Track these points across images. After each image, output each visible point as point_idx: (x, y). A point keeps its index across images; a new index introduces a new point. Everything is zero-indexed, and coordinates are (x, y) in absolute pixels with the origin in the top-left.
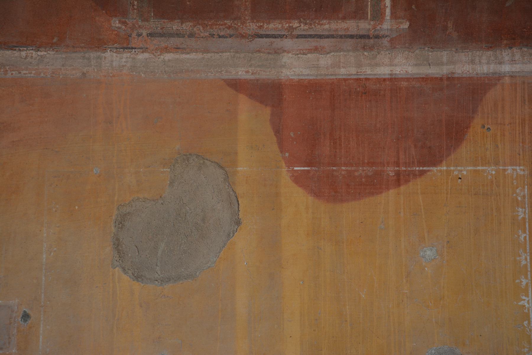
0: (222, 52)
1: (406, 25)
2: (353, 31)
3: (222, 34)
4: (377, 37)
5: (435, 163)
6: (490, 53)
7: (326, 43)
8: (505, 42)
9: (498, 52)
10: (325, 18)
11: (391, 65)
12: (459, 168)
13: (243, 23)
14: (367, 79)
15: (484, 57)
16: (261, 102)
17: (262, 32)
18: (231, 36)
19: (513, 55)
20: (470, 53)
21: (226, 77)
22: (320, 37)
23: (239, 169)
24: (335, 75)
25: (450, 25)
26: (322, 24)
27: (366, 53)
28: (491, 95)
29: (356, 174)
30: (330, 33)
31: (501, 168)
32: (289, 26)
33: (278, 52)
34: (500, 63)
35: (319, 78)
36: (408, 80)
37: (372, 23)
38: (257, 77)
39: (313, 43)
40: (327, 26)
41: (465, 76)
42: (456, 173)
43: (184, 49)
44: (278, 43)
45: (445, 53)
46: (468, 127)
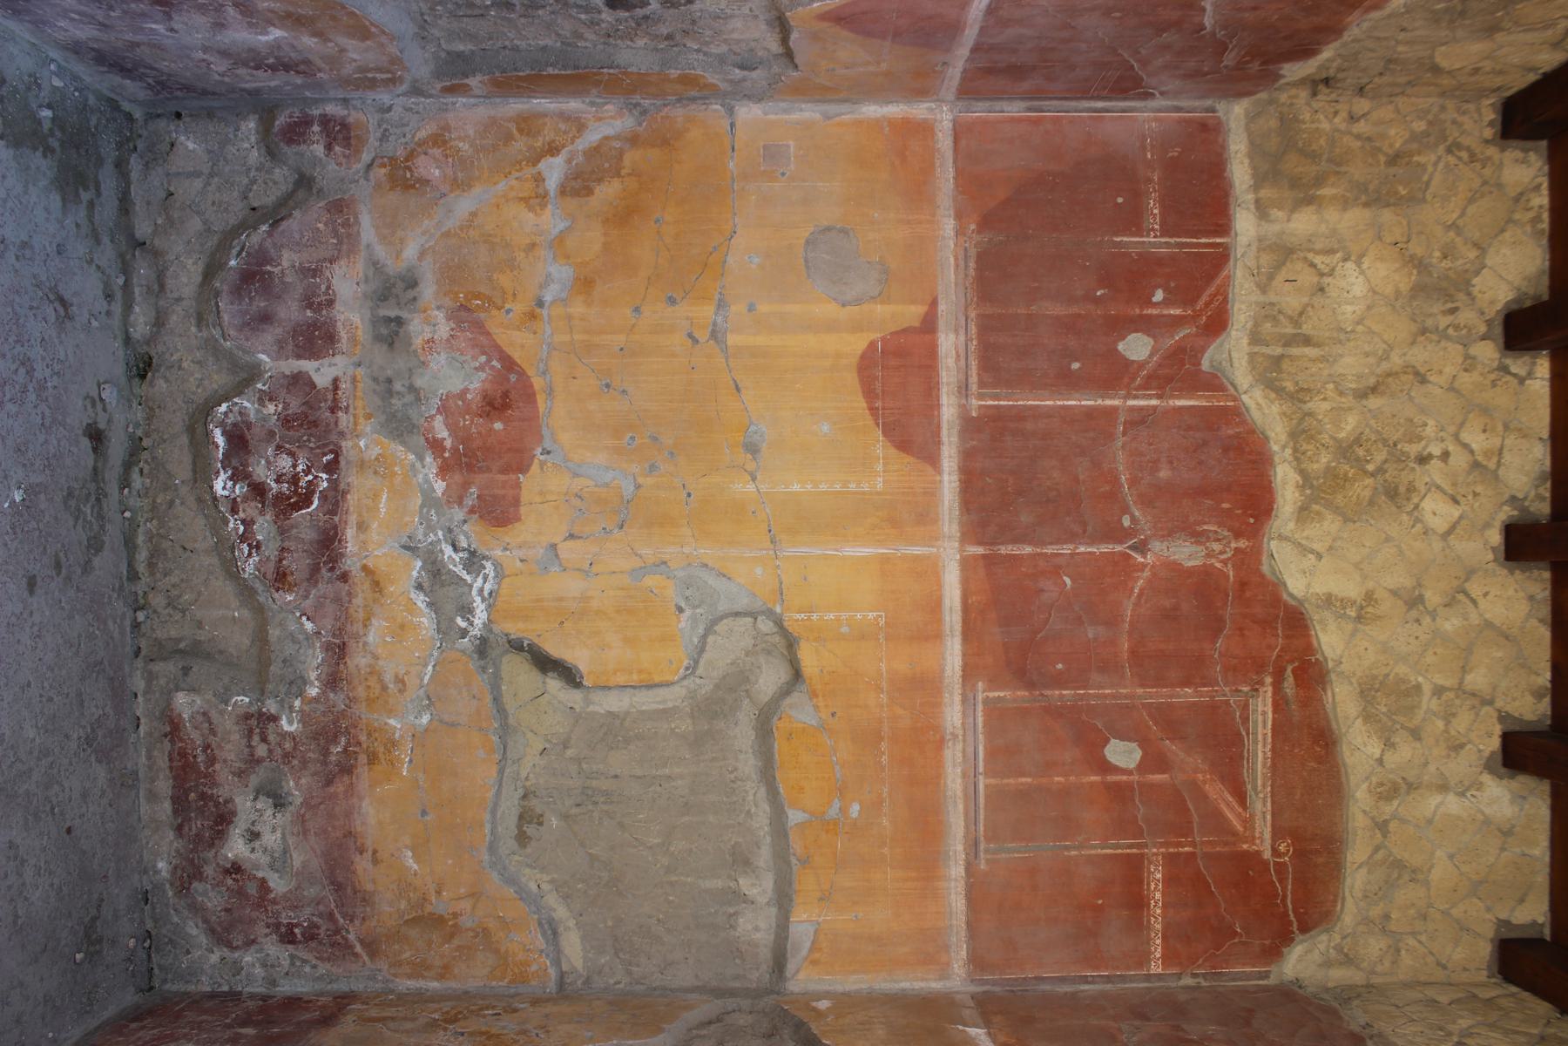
1: (974, 414)
2: (970, 380)
4: (967, 396)
5: (884, 433)
6: (956, 468)
7: (963, 362)
17: (969, 321)
18: (966, 301)
22: (967, 359)
23: (879, 306)
28: (930, 469)
33: (956, 331)
39: (962, 354)
44: (962, 331)
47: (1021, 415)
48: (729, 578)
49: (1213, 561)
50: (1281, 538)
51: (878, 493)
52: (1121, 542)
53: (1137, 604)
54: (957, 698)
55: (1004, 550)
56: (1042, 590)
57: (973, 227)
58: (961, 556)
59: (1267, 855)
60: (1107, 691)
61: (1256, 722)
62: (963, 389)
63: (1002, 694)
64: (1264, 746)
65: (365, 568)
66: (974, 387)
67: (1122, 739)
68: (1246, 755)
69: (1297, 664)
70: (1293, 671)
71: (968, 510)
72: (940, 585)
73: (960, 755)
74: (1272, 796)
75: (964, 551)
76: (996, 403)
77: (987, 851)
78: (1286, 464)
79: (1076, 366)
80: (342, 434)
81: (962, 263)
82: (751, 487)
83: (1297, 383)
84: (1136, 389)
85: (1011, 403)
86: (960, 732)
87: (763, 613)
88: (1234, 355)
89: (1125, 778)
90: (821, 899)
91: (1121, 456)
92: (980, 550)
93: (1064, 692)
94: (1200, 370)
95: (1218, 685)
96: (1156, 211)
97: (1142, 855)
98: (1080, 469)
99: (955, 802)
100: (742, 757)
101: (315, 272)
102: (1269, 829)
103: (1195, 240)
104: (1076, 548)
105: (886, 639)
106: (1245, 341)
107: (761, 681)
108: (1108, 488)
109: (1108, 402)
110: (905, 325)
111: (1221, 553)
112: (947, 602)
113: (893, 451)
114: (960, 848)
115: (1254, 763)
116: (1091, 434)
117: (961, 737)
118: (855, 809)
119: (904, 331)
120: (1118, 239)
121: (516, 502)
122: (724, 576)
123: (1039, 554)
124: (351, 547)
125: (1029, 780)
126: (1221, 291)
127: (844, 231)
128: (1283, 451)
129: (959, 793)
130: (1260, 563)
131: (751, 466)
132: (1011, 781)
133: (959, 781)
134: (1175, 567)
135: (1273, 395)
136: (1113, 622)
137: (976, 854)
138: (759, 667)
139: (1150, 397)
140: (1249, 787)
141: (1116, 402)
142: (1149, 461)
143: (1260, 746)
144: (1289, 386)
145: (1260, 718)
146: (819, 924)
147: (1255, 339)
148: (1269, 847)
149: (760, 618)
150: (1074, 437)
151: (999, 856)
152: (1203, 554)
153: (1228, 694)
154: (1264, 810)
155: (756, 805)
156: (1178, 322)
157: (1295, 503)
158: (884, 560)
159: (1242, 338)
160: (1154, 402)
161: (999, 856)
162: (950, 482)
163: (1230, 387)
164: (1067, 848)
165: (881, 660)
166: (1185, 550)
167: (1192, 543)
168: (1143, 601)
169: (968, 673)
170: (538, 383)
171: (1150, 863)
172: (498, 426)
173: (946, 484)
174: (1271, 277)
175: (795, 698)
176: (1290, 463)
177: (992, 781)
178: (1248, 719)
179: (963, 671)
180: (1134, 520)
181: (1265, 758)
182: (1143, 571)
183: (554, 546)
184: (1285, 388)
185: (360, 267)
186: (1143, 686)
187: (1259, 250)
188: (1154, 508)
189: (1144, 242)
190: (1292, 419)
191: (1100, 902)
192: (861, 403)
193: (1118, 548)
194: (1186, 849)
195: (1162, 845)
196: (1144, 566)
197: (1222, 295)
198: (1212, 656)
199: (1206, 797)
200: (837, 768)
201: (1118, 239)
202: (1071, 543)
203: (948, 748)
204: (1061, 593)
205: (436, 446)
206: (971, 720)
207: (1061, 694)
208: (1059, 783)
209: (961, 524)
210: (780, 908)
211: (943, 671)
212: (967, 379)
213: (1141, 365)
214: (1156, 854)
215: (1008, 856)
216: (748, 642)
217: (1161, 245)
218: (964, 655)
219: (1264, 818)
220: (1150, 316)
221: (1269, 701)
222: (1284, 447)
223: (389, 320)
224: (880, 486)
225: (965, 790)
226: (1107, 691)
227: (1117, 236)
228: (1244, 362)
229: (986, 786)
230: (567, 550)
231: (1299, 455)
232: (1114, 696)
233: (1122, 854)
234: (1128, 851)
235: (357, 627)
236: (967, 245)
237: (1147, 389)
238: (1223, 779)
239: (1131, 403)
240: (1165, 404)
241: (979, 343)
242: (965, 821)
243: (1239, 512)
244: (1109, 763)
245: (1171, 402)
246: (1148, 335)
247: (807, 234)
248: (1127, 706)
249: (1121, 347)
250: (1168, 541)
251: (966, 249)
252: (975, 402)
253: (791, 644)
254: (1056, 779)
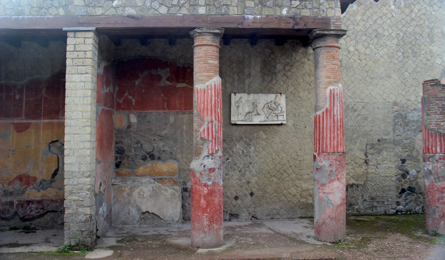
55: (42, 114)
62: (22, 119)
65: (42, 197)
72: (46, 122)
80: (24, 200)
92: (42, 117)
101: (3, 204)
121: (34, 177)
124: (38, 199)
158: (43, 130)
169: (58, 119)
170: (19, 174)
172: (24, 179)
183: (40, 172)
185: (2, 198)
192: (23, 133)
205: (26, 187)
223: (10, 194)
230: (40, 170)
235: (49, 198)
252: (24, 118)
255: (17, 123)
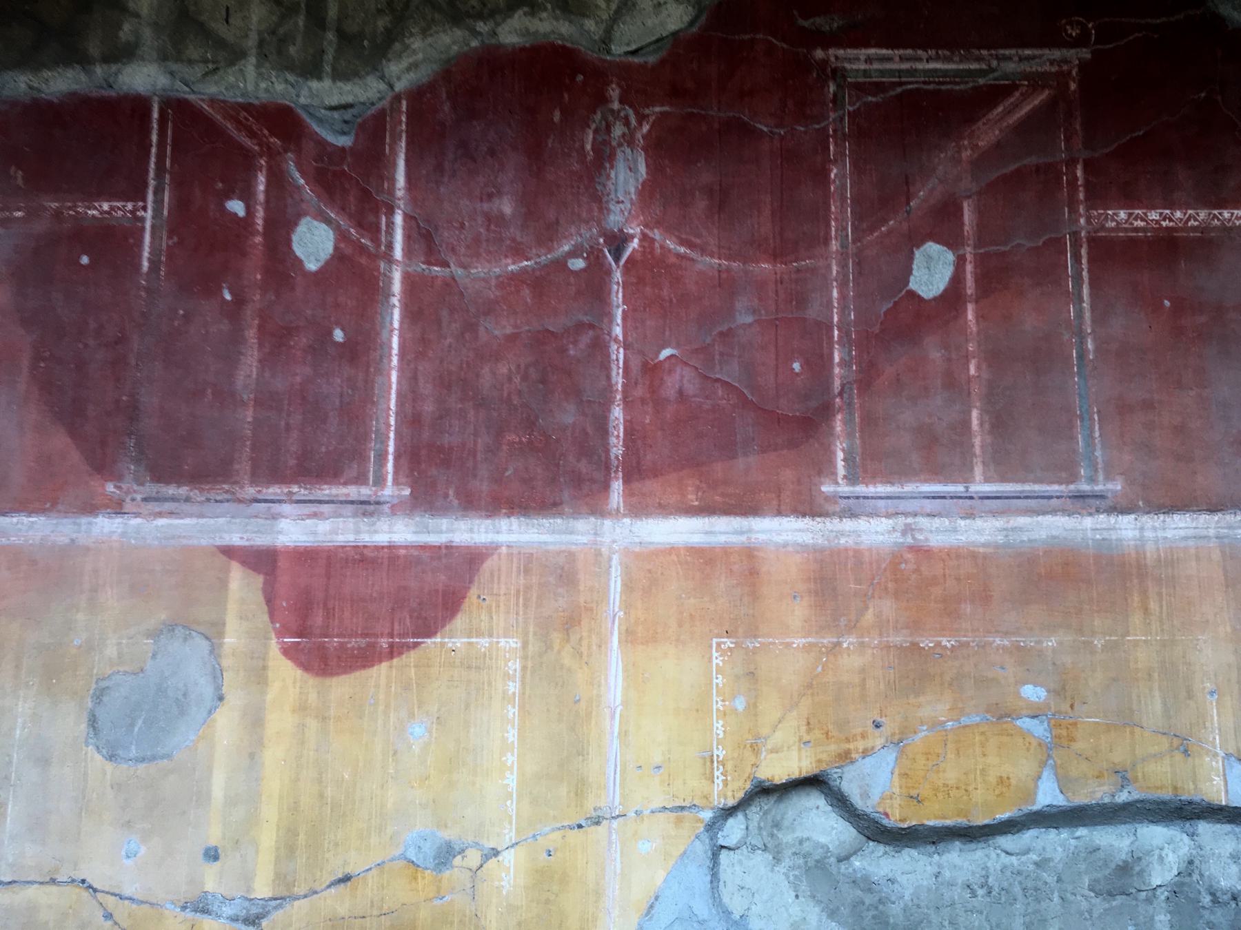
0: (217, 517)
1: (407, 492)
2: (354, 497)
3: (219, 498)
4: (378, 503)
5: (430, 634)
6: (489, 521)
7: (325, 508)
8: (504, 511)
9: (497, 521)
10: (326, 483)
11: (390, 532)
12: (453, 640)
13: (242, 488)
14: (365, 547)
15: (483, 526)
16: (255, 570)
17: (260, 497)
18: (228, 501)
19: (511, 525)
20: (469, 522)
21: (219, 542)
22: (320, 502)
23: (226, 640)
24: (333, 542)
25: (451, 492)
26: (323, 490)
27: (365, 520)
28: (488, 564)
29: (349, 646)
30: (331, 499)
31: (495, 640)
32: (289, 491)
33: (275, 517)
34: (498, 533)
35: (316, 544)
36: (406, 547)
37: (374, 489)
38: (252, 543)
40: (327, 492)
41: (463, 544)
42: (450, 645)
43: (178, 514)
44: (276, 508)
45: (445, 521)
46: (464, 597)
47: (411, 420)
48: (657, 898)
49: (639, 136)
50: (607, 39)
51: (525, 645)
52: (609, 272)
53: (703, 251)
54: (848, 524)
55: (617, 449)
56: (681, 392)
57: (110, 487)
58: (625, 516)
59: (1085, 54)
60: (835, 294)
61: (882, 73)
62: (367, 508)
63: (840, 455)
64: (919, 59)
66: (365, 492)
67: (909, 271)
68: (931, 87)
69: (795, 12)
70: (806, 18)
71: (555, 504)
72: (672, 550)
73: (937, 522)
74: (996, 48)
75: (618, 510)
76: (391, 458)
77: (1092, 480)
78: (499, 30)
79: (338, 335)
81: (168, 506)
82: (508, 857)
83: (380, 11)
84: (379, 246)
85: (392, 435)
86: (901, 520)
87: (713, 838)
88: (335, 100)
89: (969, 268)
90: (1186, 752)
91: (479, 270)
92: (617, 486)
93: (837, 359)
94: (351, 148)
95: (825, 129)
96: (106, 207)
97: (1093, 241)
98: (497, 332)
99: (1013, 529)
100: (947, 874)
102: (1047, 51)
103: (154, 150)
104: (616, 340)
105: (755, 637)
106: (314, 84)
107: (823, 840)
108: (526, 292)
109: (397, 287)
110: (260, 598)
111: (627, 123)
112: (697, 539)
113: (460, 621)
114: (1088, 522)
115: (945, 73)
116: (445, 313)
117: (910, 520)
118: (1032, 693)
119: (270, 600)
120: (146, 264)
122: (651, 907)
123: (625, 399)
125: (975, 414)
126: (232, 113)
127: (99, 696)
128: (480, 34)
129: (999, 523)
130: (643, 66)
131: (473, 858)
132: (977, 441)
133: (979, 523)
134: (648, 192)
135: (397, 46)
136: (726, 285)
137: (1096, 496)
138: (801, 842)
139: (390, 225)
140: (981, 81)
141: (397, 276)
142: (488, 230)
143: (920, 66)
144: (382, 23)
145: (876, 66)
146: (1228, 756)
147: (311, 69)
148: (1073, 51)
149: (721, 842)
150: (449, 340)
151: (1100, 460)
152: (628, 151)
153: (841, 112)
154: (1016, 59)
155: (1027, 851)
156: (277, 180)
157: (557, 19)
158: (629, 637)
159: (310, 89)
160: (399, 219)
161: (1100, 460)
162: (510, 531)
163: (379, 106)
164: (1082, 356)
165: (788, 645)
166: (621, 178)
167: (612, 167)
168: (698, 241)
169: (809, 507)
171: (1103, 228)
173: (513, 538)
174: (221, 44)
175: (850, 787)
176: (498, 24)
177: (978, 471)
178: (877, 84)
179: (804, 515)
180: (574, 254)
181: (937, 58)
182: (653, 240)
184: (386, 29)
186: (826, 241)
187: (178, 59)
188: (557, 222)
189: (153, 227)
190: (433, 20)
191: (1167, 303)
193: (618, 276)
194: (1079, 173)
195: (1073, 210)
196: (644, 237)
197: (238, 114)
198: (782, 138)
199: (998, 145)
200: (965, 720)
201: (145, 264)
202: (608, 347)
203: (927, 540)
204: (686, 364)
206: (881, 503)
207: (840, 365)
208: (978, 368)
209: (576, 514)
210: (1199, 818)
211: (804, 548)
212: (352, 502)
213: (342, 236)
214: (1088, 221)
215: (1099, 446)
216: (760, 860)
217: (158, 202)
218: (779, 513)
219: (1028, 58)
220: (267, 221)
221: (851, 52)
222: (475, 33)
224: (514, 643)
225: (995, 514)
226: (835, 294)
227: (140, 265)
228: (347, 87)
229: (987, 480)
231: (486, 11)
232: (843, 286)
233: (1089, 271)
234: (1084, 261)
236: (139, 497)
237: (378, 230)
238: (971, 120)
239: (398, 253)
240: (401, 203)
241: (297, 482)
242: (1044, 513)
243: (566, 96)
244: (946, 291)
245: (400, 193)
246: (296, 224)
247: (98, 757)
248: (858, 264)
249: (312, 266)
250: (607, 202)
251: (145, 500)
252: (389, 491)
253: (764, 791)
254: (972, 371)
255: (305, 556)
